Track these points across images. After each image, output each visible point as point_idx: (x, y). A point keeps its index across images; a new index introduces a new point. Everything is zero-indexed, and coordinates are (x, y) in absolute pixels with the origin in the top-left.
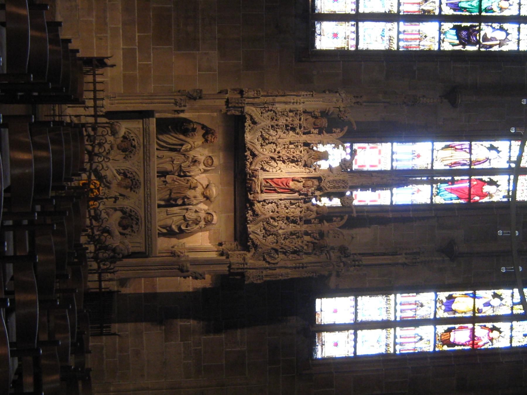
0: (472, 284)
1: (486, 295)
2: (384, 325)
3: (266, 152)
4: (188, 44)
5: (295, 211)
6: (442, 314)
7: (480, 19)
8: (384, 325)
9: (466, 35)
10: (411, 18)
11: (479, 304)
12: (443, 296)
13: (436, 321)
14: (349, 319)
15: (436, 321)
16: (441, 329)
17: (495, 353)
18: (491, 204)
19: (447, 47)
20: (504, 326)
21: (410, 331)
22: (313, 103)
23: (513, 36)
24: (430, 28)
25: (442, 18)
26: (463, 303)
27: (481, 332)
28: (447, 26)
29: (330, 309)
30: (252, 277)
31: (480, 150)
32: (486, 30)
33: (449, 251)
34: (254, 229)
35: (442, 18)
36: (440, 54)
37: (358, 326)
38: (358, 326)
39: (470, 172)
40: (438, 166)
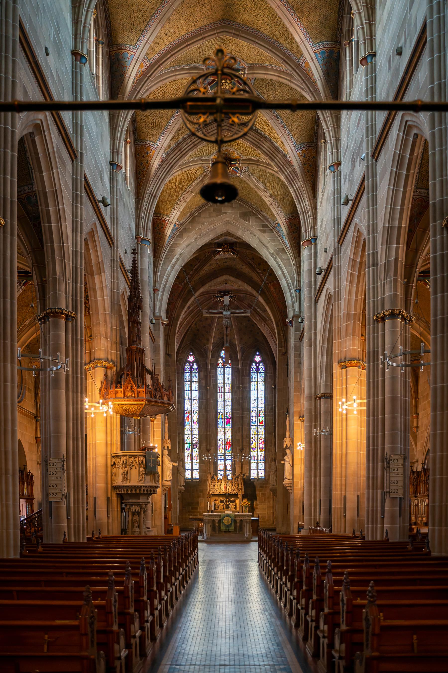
0: (249, 444)
1: (252, 440)
2: (258, 463)
3: (219, 491)
4: (198, 503)
5: (230, 485)
6: (256, 450)
7: (192, 443)
8: (258, 463)
9: (195, 446)
10: (192, 459)
11: (254, 442)
12: (252, 450)
13: (257, 452)
14: (256, 471)
15: (257, 452)
16: (259, 450)
17: (265, 438)
18: (232, 440)
19: (198, 451)
20: (259, 436)
21: (259, 457)
22: (209, 481)
23: (195, 436)
24: (194, 454)
25: (192, 452)
26: (254, 446)
27: (260, 441)
28: (193, 451)
29: (254, 474)
30: (243, 493)
31: (220, 443)
32: (194, 442)
33: (242, 450)
34: (234, 492)
35: (192, 452)
36: (199, 452)
37: (258, 469)
38: (258, 469)
39: (225, 445)
40: (223, 452)
